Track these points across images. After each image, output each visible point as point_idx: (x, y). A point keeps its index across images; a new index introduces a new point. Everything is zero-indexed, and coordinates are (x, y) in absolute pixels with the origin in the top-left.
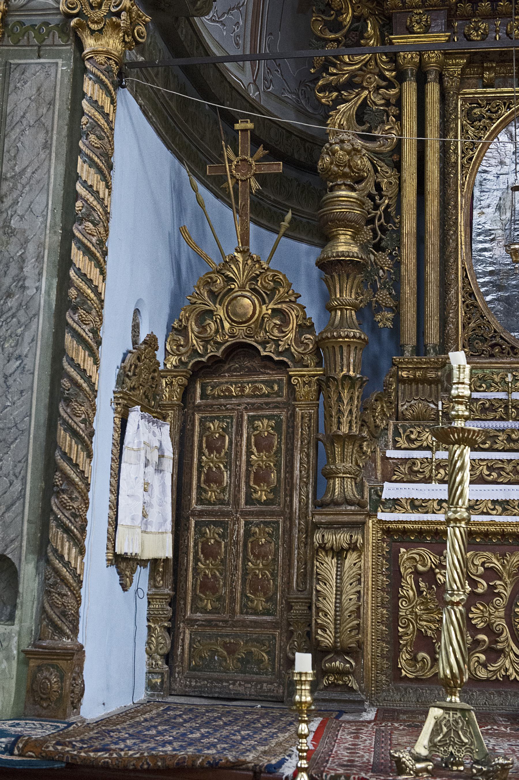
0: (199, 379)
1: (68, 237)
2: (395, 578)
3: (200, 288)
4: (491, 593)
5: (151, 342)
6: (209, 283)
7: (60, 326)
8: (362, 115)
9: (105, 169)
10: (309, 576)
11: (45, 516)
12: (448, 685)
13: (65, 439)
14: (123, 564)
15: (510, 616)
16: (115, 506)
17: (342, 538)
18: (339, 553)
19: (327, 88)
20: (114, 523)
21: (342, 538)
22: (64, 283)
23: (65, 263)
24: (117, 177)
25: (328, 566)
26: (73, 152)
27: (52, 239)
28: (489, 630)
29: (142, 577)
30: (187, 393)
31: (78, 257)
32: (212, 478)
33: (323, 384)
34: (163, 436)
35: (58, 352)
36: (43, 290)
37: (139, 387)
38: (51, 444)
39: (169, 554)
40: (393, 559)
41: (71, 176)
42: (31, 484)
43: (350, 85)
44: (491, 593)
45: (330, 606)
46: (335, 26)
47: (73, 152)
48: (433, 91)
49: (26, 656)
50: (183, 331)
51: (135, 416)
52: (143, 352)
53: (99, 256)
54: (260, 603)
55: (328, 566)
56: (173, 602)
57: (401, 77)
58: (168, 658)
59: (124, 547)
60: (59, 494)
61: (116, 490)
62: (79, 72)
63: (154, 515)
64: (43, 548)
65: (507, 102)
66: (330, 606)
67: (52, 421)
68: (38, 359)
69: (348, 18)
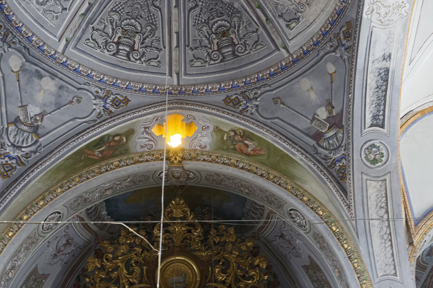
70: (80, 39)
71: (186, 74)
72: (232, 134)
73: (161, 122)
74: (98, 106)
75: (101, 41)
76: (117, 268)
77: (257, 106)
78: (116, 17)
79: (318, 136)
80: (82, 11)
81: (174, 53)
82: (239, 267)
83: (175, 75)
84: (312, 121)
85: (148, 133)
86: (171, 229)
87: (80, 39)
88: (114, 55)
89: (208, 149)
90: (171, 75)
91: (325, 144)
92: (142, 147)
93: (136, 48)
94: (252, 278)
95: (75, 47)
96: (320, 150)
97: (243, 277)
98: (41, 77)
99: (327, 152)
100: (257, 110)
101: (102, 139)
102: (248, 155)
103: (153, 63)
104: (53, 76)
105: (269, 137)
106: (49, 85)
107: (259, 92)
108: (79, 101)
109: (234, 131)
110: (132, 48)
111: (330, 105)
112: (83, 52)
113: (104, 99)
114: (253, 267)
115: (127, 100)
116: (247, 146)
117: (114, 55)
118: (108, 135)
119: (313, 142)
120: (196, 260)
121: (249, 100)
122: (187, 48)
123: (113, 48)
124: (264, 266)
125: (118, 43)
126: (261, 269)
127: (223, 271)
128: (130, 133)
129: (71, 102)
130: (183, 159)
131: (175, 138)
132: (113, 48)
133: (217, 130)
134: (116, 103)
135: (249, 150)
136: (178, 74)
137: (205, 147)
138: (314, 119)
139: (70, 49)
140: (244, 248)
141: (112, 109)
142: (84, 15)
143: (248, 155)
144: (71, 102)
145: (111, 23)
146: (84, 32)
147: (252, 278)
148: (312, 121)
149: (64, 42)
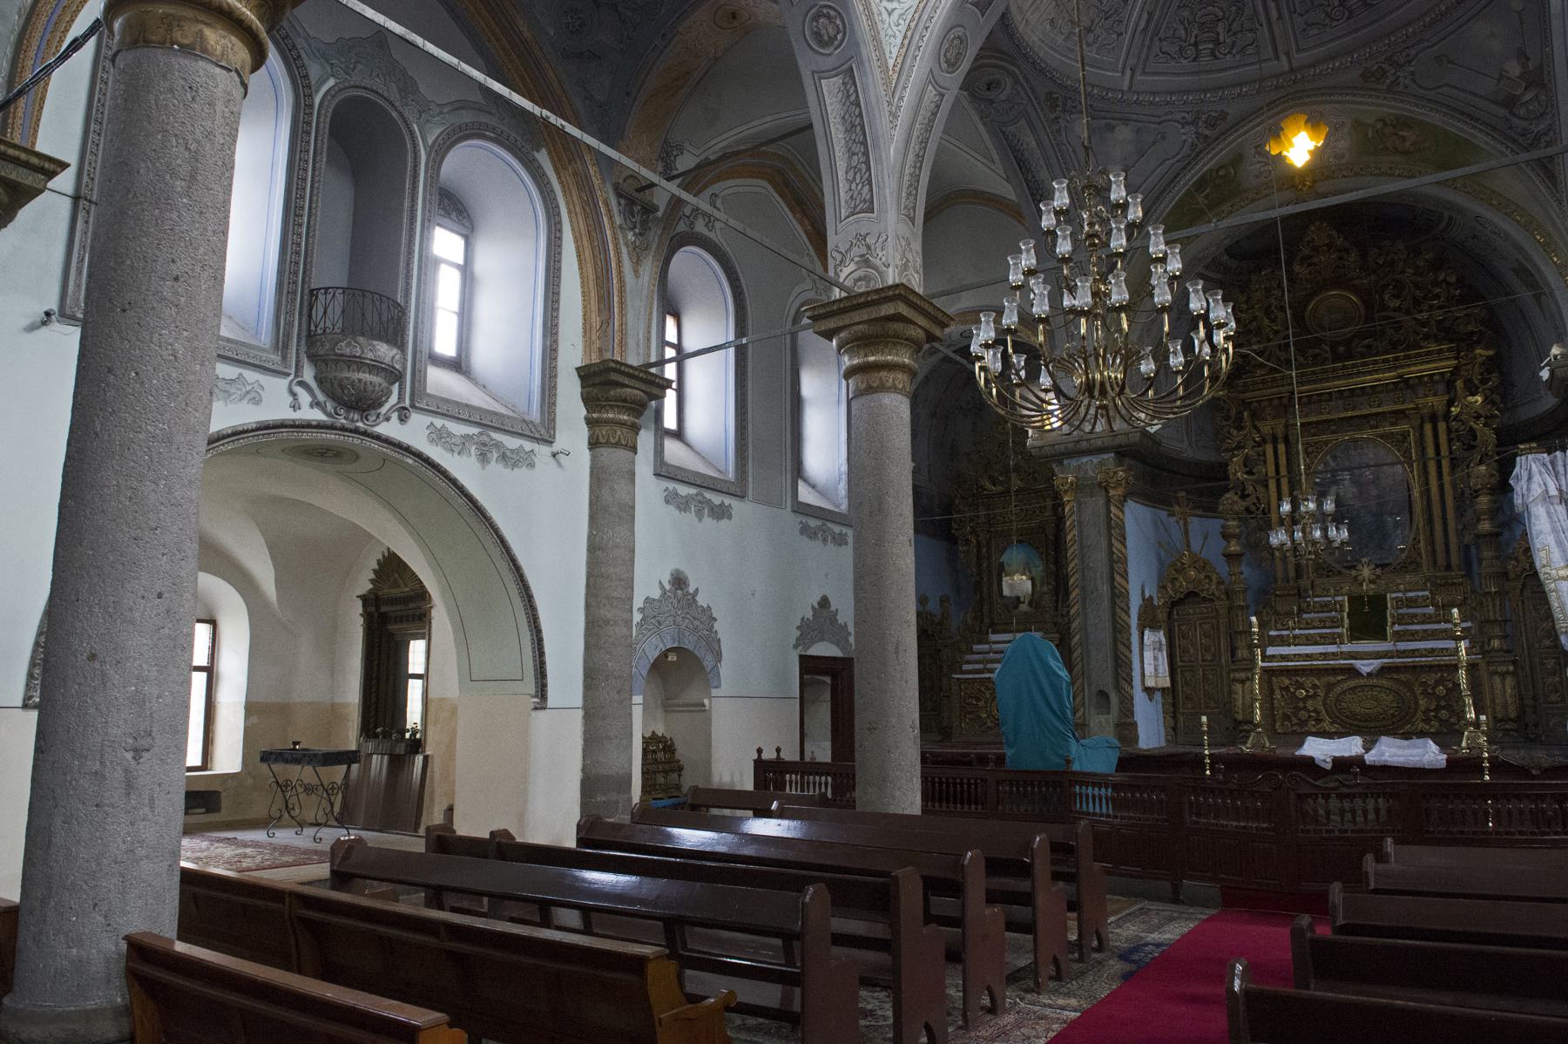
0: (1170, 612)
1: (1112, 568)
2: (1272, 691)
3: (1169, 571)
4: (1315, 695)
5: (1151, 598)
6: (1173, 565)
7: (1113, 603)
8: (1246, 462)
9: (1123, 540)
10: (1230, 692)
11: (1117, 675)
12: (1257, 726)
13: (1122, 648)
14: (1149, 691)
15: (1324, 704)
16: (1143, 668)
17: (1242, 675)
18: (1242, 682)
19: (1227, 450)
20: (1143, 675)
21: (1242, 675)
22: (1113, 587)
23: (1112, 579)
24: (1129, 543)
25: (1238, 687)
26: (1110, 535)
27: (1106, 570)
28: (1315, 711)
29: (1158, 696)
30: (1170, 614)
31: (1118, 578)
32: (1185, 651)
33: (1230, 609)
34: (1161, 636)
35: (1114, 614)
36: (1105, 589)
37: (1148, 620)
38: (1115, 649)
39: (1167, 683)
40: (1270, 683)
41: (1110, 545)
42: (1110, 663)
43: (1239, 447)
44: (1315, 695)
45: (1240, 703)
46: (1227, 418)
47: (1110, 535)
48: (1282, 448)
49: (1117, 725)
50: (1165, 587)
51: (1147, 632)
52: (1147, 604)
53: (1125, 576)
54: (1212, 704)
55: (1238, 687)
56: (1174, 705)
57: (1264, 440)
58: (1174, 729)
59: (1150, 683)
60: (1121, 667)
61: (1142, 662)
62: (1108, 502)
63: (1161, 670)
64: (1117, 687)
65: (1326, 443)
66: (1240, 703)
67: (1115, 640)
68: (1106, 616)
69: (1233, 412)
70: (1146, 60)
71: (1299, 50)
72: (1380, 125)
73: (1276, 133)
74: (1188, 134)
75: (1173, 49)
76: (1255, 318)
77: (1412, 73)
78: (1186, 13)
79: (1510, 103)
80: (1142, 24)
81: (1275, 28)
82: (1417, 286)
83: (1284, 58)
84: (1499, 81)
85: (1260, 154)
86: (1315, 260)
87: (1146, 60)
88: (1194, 60)
89: (1343, 161)
90: (1278, 58)
91: (1522, 112)
92: (1257, 177)
93: (1221, 39)
94: (1437, 296)
95: (1144, 73)
96: (1515, 121)
97: (1425, 297)
98: (1112, 128)
99: (1525, 123)
100: (1414, 81)
101: (1202, 178)
102: (1406, 153)
103: (1250, 50)
104: (1126, 121)
105: (1436, 119)
106: (1124, 133)
107: (1413, 52)
108: (1163, 138)
109: (1383, 120)
110: (1217, 42)
111: (1522, 55)
112: (1155, 74)
113: (1194, 123)
114: (1436, 284)
115: (1224, 115)
116: (1404, 139)
117: (1194, 60)
118: (1210, 170)
119: (1503, 112)
120: (1356, 290)
121: (1400, 66)
122: (1295, 16)
123: (1191, 52)
124: (1453, 279)
125: (1196, 44)
126: (1449, 284)
127: (1397, 296)
128: (1237, 160)
129: (1154, 143)
130: (1314, 182)
131: (1300, 148)
132: (1191, 52)
133: (1358, 125)
134: (1210, 123)
135: (1408, 144)
136: (1287, 54)
137: (1343, 156)
138: (1501, 77)
139: (1138, 77)
140: (1421, 263)
141: (1207, 132)
142: (1145, 29)
143: (1406, 153)
144: (1154, 143)
145: (1182, 23)
146: (1149, 48)
147: (1437, 296)
148: (1499, 81)
149: (1128, 72)
